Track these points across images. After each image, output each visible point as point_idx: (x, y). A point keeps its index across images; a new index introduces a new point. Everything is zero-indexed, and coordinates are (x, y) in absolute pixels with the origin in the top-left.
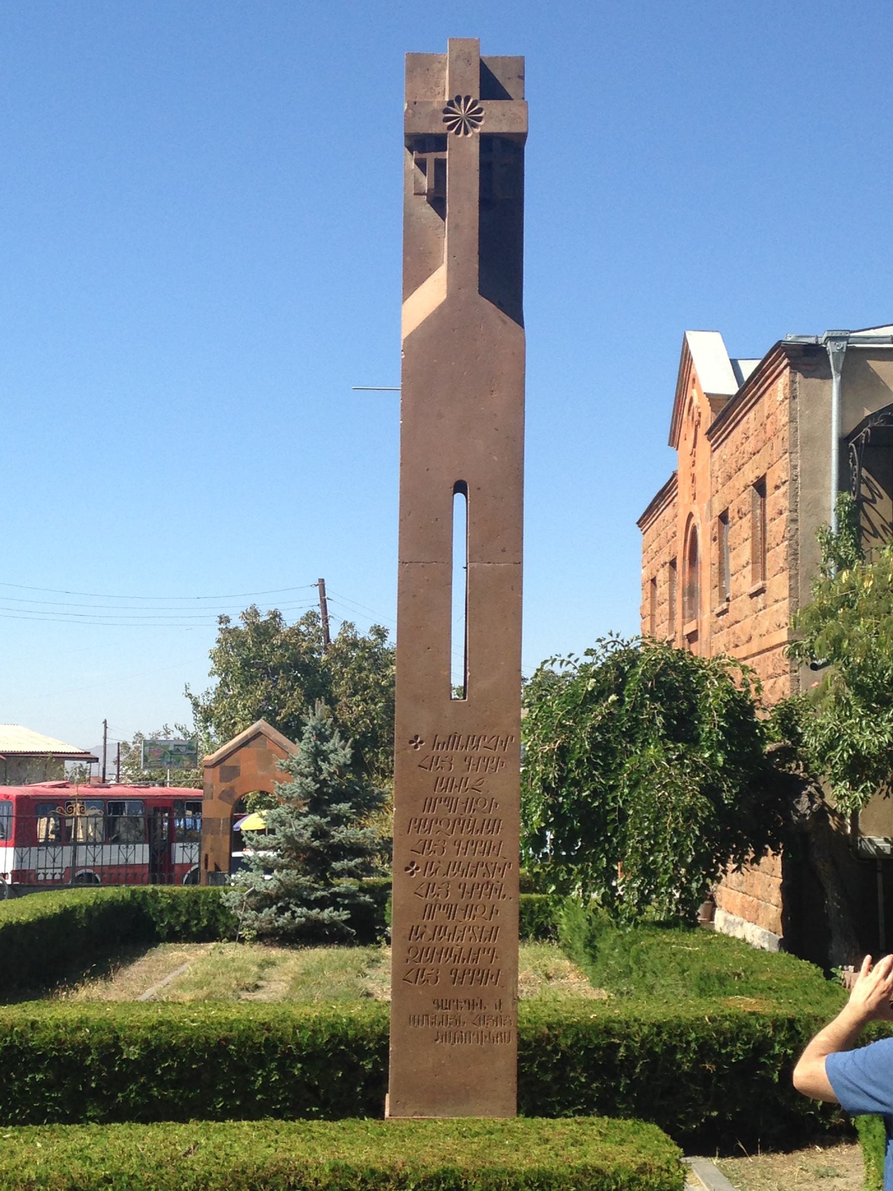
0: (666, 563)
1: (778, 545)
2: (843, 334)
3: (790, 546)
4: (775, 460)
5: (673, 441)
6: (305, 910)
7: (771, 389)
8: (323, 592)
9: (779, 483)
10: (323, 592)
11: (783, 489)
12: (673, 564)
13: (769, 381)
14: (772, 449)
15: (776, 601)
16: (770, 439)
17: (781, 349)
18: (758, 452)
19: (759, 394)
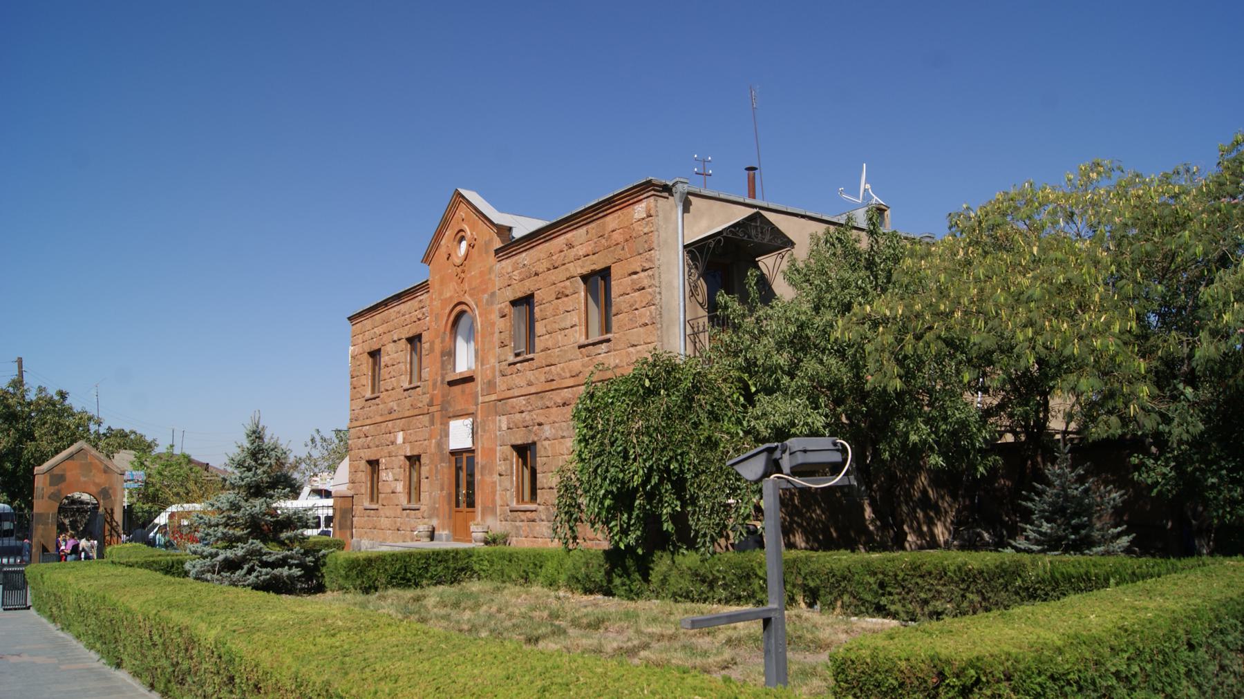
0: (399, 340)
1: (636, 309)
2: (685, 181)
3: (656, 309)
4: (629, 256)
5: (427, 258)
6: (269, 569)
7: (619, 212)
8: (20, 366)
9: (639, 269)
10: (20, 366)
11: (642, 274)
12: (415, 340)
13: (617, 208)
14: (623, 249)
15: (634, 346)
16: (617, 244)
17: (647, 186)
18: (594, 254)
19: (595, 217)
